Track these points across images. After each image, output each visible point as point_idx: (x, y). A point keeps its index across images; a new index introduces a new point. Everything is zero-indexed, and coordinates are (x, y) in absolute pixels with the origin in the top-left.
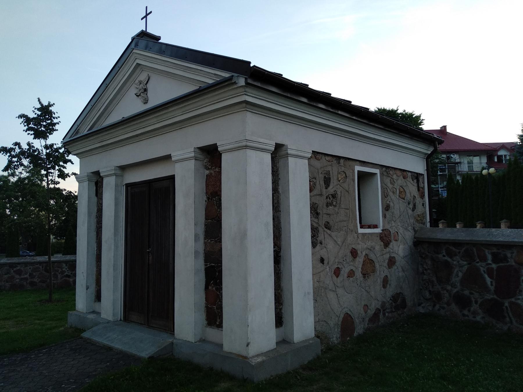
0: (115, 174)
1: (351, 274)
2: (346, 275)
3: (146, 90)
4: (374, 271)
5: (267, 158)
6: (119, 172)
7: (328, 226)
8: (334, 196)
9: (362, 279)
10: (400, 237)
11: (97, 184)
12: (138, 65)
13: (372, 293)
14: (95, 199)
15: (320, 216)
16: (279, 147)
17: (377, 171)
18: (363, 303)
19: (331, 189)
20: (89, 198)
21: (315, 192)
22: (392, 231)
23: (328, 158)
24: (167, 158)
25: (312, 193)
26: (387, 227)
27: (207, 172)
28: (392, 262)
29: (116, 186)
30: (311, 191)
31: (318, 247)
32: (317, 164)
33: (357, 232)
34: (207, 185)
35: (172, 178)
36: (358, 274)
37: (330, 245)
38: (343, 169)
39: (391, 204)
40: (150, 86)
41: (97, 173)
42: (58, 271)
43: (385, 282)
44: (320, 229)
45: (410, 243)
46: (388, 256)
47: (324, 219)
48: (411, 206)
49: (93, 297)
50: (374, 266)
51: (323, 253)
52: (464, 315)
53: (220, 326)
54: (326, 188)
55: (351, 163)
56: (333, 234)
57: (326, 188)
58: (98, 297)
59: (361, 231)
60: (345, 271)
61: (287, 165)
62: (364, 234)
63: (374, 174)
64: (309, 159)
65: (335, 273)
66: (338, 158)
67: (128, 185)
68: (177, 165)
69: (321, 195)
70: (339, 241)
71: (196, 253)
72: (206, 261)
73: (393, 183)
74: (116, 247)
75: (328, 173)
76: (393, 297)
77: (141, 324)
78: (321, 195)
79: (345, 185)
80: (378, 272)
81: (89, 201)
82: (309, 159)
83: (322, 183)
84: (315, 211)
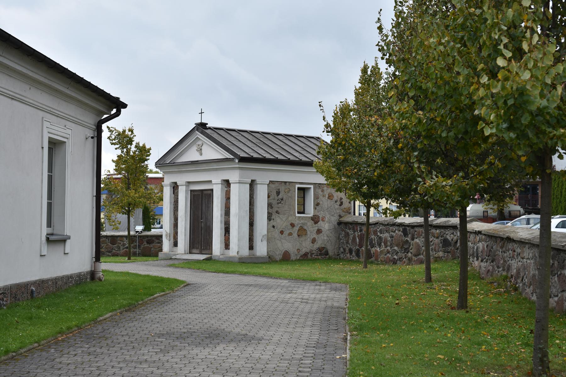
0: (185, 185)
1: (290, 234)
2: (287, 234)
3: (201, 149)
4: (306, 234)
5: (248, 186)
6: (187, 184)
7: (277, 212)
8: (282, 199)
9: (297, 237)
10: (327, 219)
11: (174, 188)
12: (197, 137)
13: (304, 245)
14: (173, 195)
15: (273, 208)
16: (253, 181)
17: (312, 186)
18: (297, 248)
19: (280, 196)
20: (170, 195)
21: (271, 198)
22: (321, 216)
23: (279, 183)
24: (210, 182)
25: (269, 199)
26: (318, 214)
27: (226, 189)
28: (319, 231)
29: (186, 191)
30: (269, 197)
31: (272, 221)
32: (272, 186)
33: (295, 216)
34: (226, 195)
35: (212, 190)
36: (295, 235)
37: (279, 220)
38: (288, 187)
39: (321, 203)
40: (203, 148)
41: (176, 183)
42: (120, 244)
43: (314, 241)
44: (273, 213)
45: (336, 223)
46: (317, 228)
47: (275, 209)
48: (338, 203)
49: (173, 244)
50: (307, 232)
51: (274, 224)
52: (351, 258)
53: (229, 249)
54: (277, 196)
55: (293, 184)
56: (281, 216)
57: (277, 196)
58: (176, 244)
59: (297, 215)
60: (286, 233)
61: (257, 188)
62: (299, 217)
63: (310, 188)
64: (268, 185)
65: (280, 233)
66: (285, 182)
67: (191, 191)
68: (214, 185)
69: (274, 199)
70: (284, 219)
71: (221, 221)
72: (225, 225)
73: (323, 191)
74: (186, 220)
75: (279, 190)
76: (319, 248)
77: (198, 254)
78: (274, 199)
79: (289, 194)
80: (309, 236)
81: (170, 197)
82: (268, 185)
83: (275, 194)
84: (270, 205)
